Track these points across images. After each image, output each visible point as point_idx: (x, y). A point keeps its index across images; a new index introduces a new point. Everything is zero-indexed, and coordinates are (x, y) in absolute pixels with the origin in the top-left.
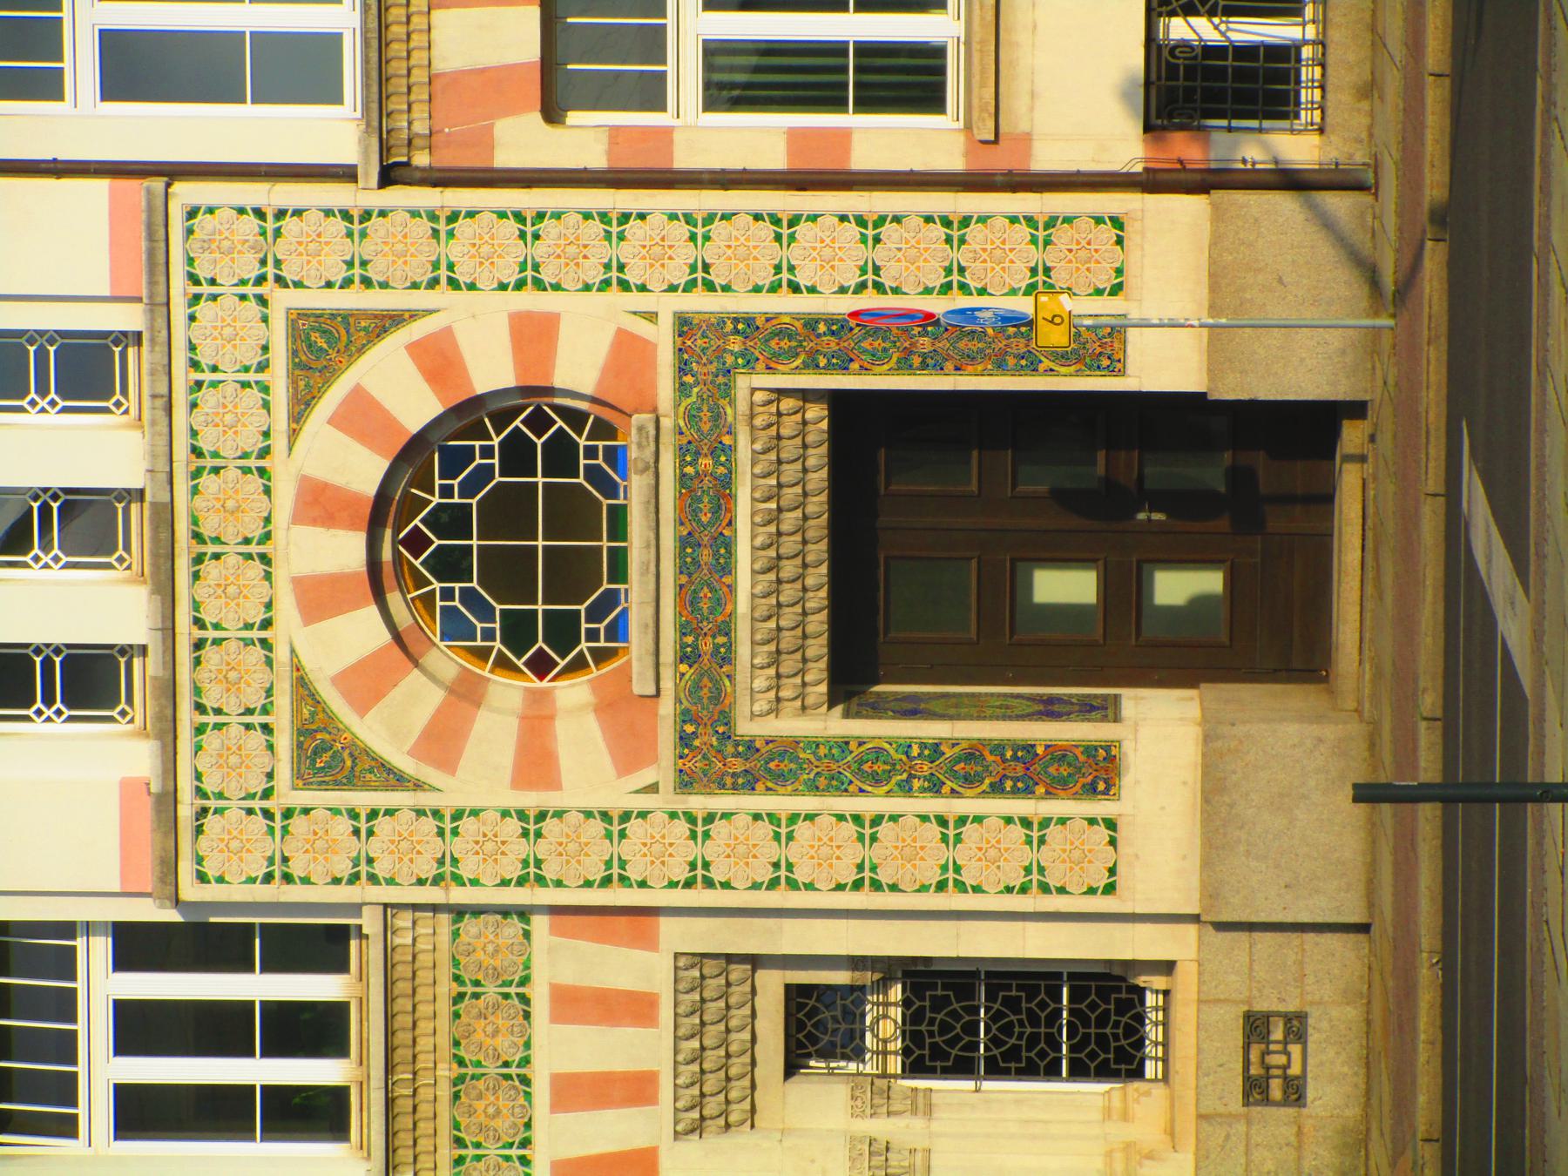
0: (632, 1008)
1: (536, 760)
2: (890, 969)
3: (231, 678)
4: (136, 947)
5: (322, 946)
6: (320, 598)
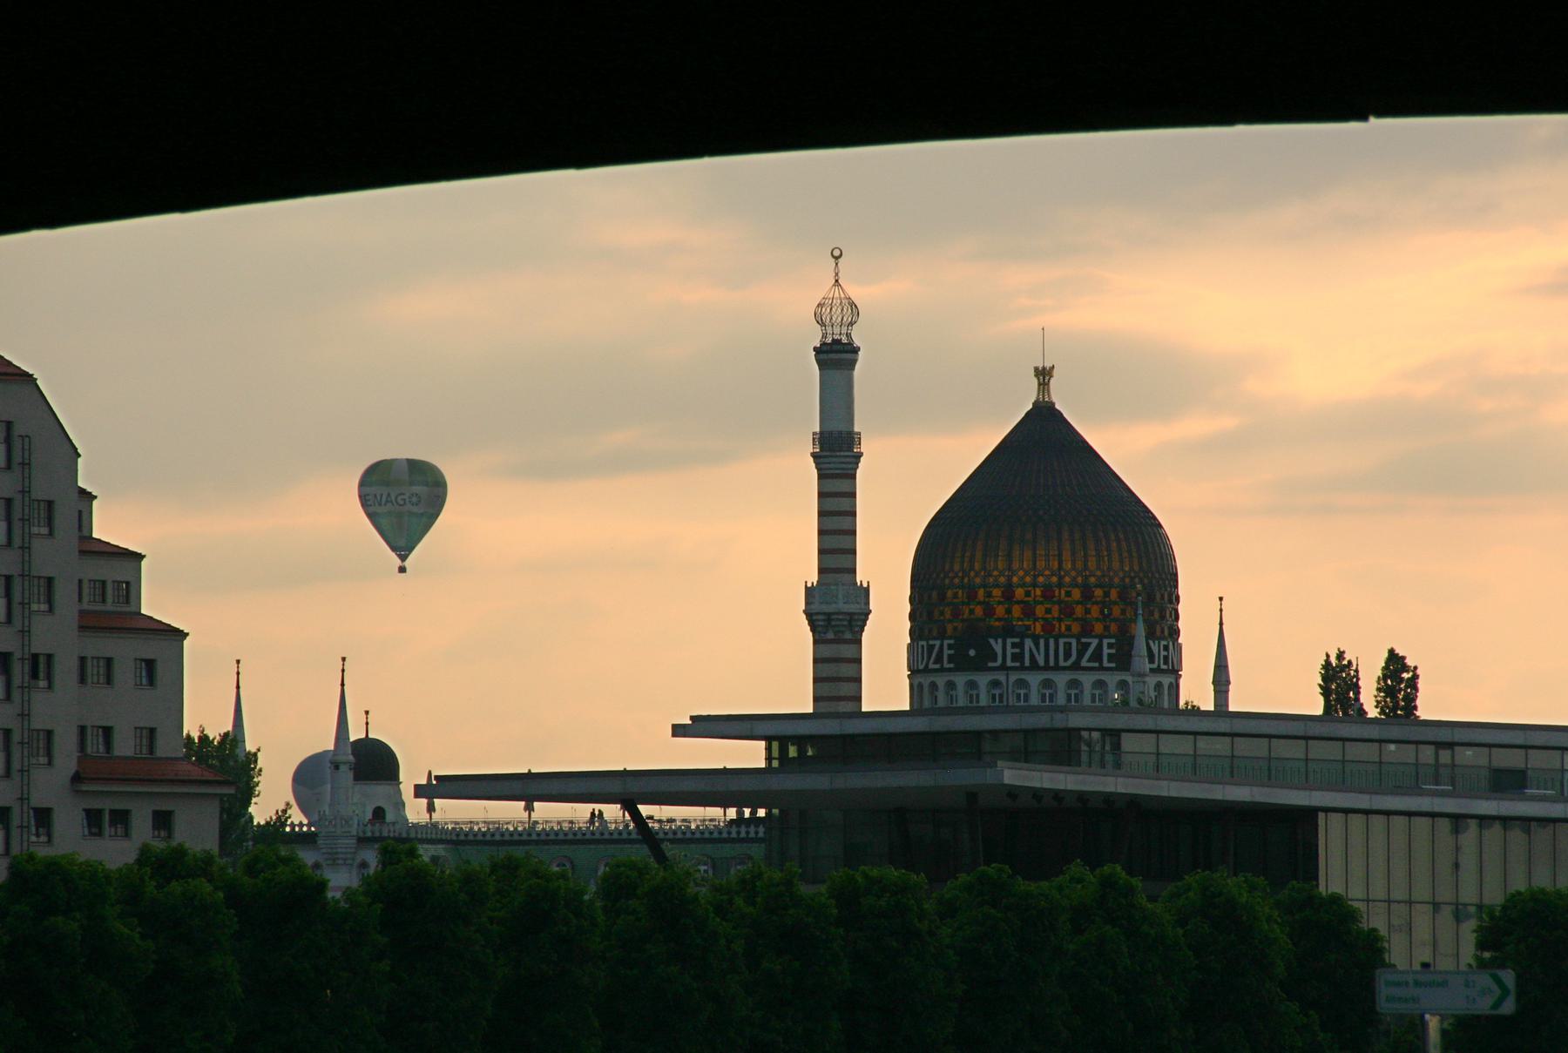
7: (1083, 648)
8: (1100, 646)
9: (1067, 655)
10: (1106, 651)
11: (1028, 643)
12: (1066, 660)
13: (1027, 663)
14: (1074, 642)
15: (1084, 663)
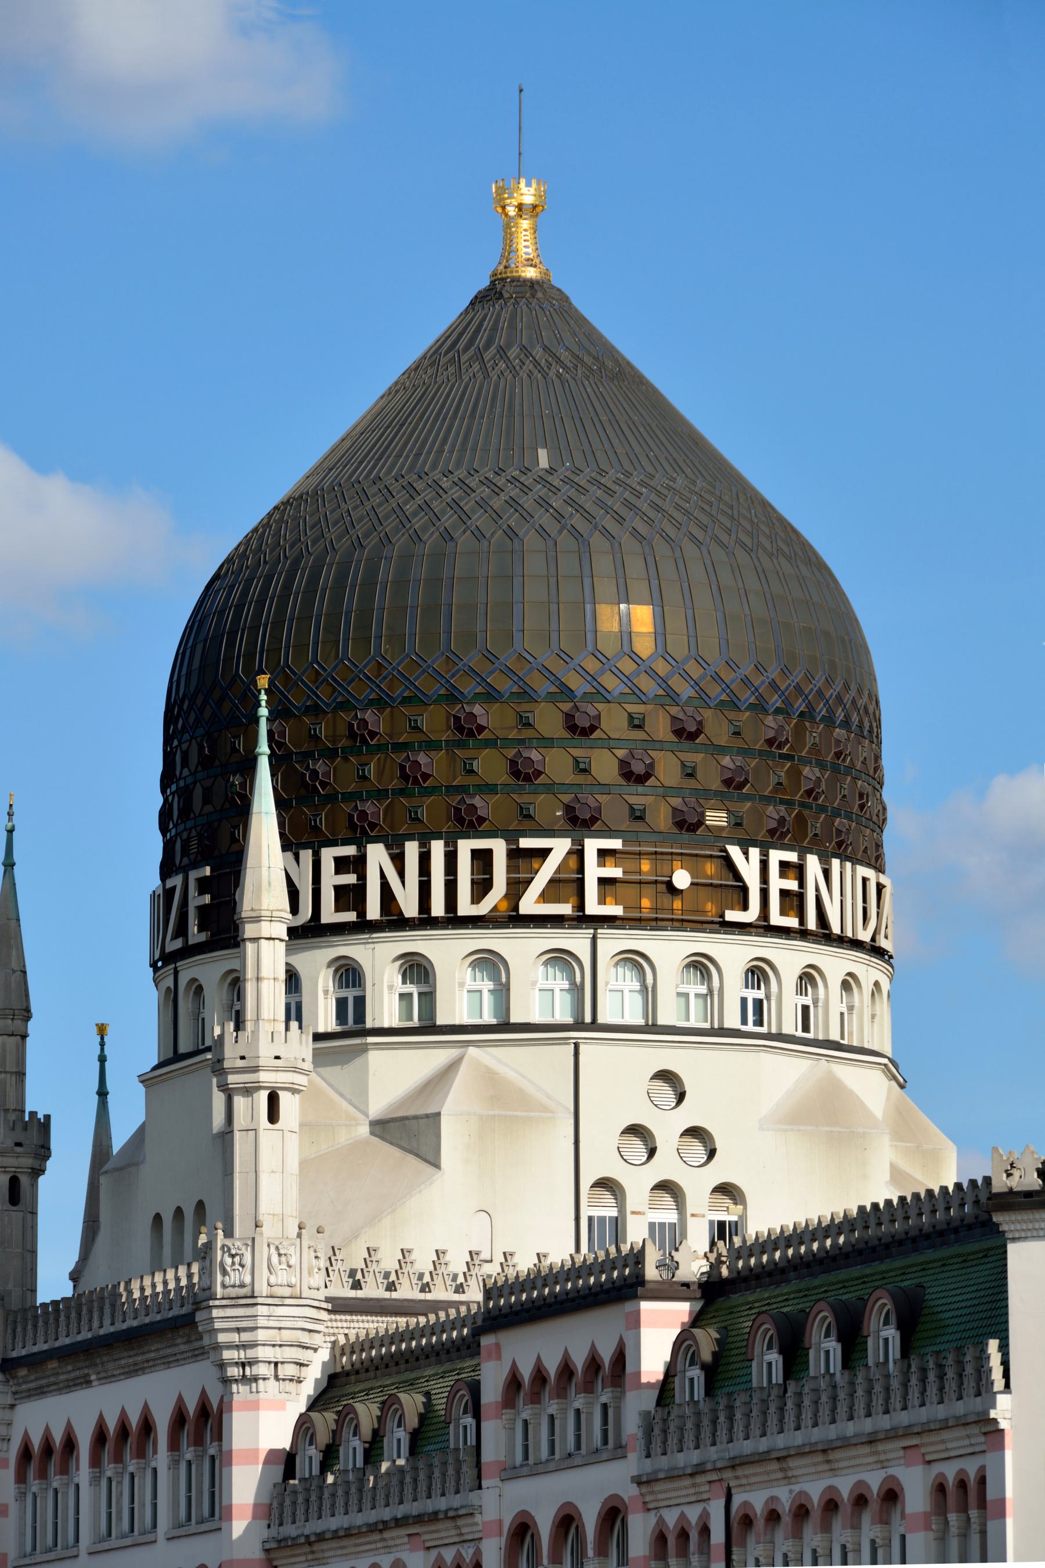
7: (523, 861)
9: (482, 887)
10: (593, 872)
11: (377, 855)
13: (373, 911)
14: (499, 847)
15: (529, 905)
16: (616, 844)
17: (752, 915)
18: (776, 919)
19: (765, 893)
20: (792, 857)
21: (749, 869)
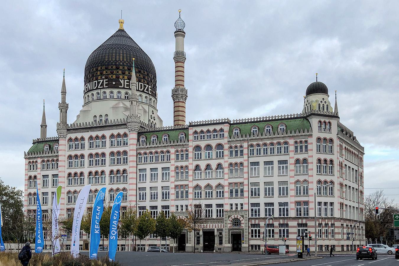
0: (221, 227)
1: (229, 224)
2: (222, 236)
3: (232, 213)
4: (223, 210)
5: (223, 216)
6: (234, 216)
7: (99, 83)
8: (103, 82)
9: (95, 86)
10: (105, 83)
12: (95, 87)
16: (107, 80)
17: (123, 86)
18: (126, 87)
19: (124, 84)
20: (128, 81)
21: (122, 82)
